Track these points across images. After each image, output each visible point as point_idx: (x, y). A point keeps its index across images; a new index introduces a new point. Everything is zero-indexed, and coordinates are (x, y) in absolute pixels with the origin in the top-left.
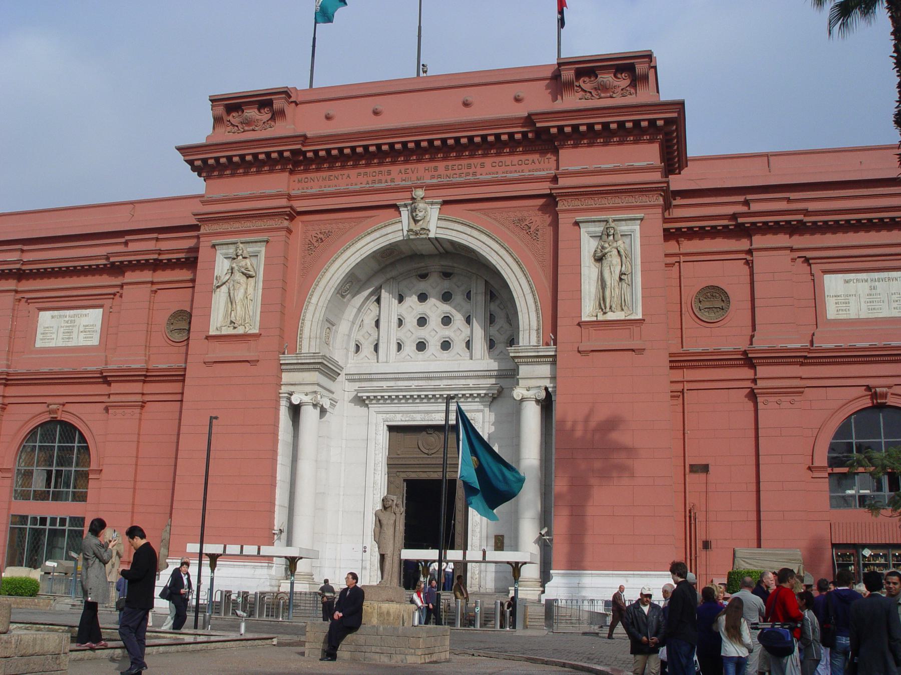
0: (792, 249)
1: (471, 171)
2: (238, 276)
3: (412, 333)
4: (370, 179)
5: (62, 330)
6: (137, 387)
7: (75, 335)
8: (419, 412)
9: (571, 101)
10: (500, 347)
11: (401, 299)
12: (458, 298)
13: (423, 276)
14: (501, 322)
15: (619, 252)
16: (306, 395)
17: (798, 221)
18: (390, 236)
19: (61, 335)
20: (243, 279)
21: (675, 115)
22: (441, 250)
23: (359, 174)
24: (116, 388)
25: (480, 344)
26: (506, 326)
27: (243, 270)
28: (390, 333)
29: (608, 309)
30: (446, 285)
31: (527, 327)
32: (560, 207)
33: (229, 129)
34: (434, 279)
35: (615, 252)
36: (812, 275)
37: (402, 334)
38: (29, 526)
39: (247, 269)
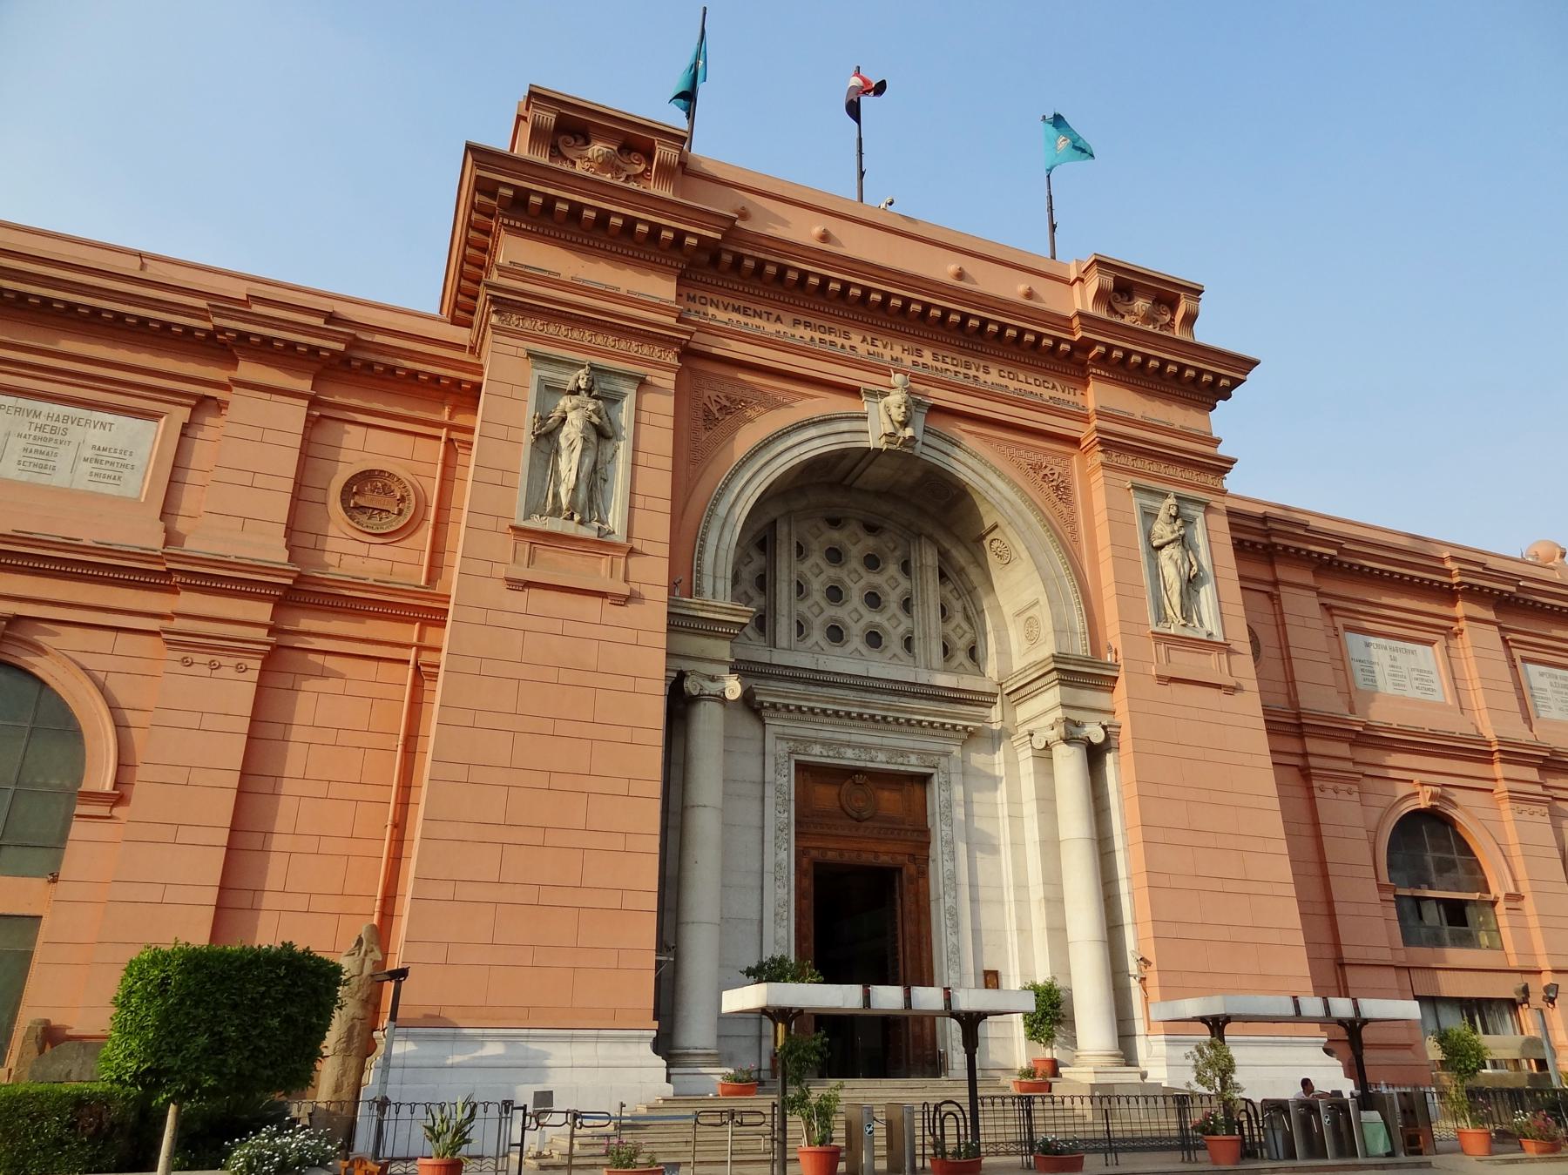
0: (1320, 594)
1: (972, 372)
4: (817, 335)
6: (262, 611)
8: (849, 745)
13: (835, 523)
14: (958, 618)
16: (713, 679)
17: (1332, 556)
18: (846, 437)
20: (593, 438)
21: (1240, 376)
23: (796, 322)
25: (937, 649)
26: (965, 626)
27: (595, 419)
30: (869, 543)
34: (854, 527)
36: (1336, 629)
37: (803, 607)
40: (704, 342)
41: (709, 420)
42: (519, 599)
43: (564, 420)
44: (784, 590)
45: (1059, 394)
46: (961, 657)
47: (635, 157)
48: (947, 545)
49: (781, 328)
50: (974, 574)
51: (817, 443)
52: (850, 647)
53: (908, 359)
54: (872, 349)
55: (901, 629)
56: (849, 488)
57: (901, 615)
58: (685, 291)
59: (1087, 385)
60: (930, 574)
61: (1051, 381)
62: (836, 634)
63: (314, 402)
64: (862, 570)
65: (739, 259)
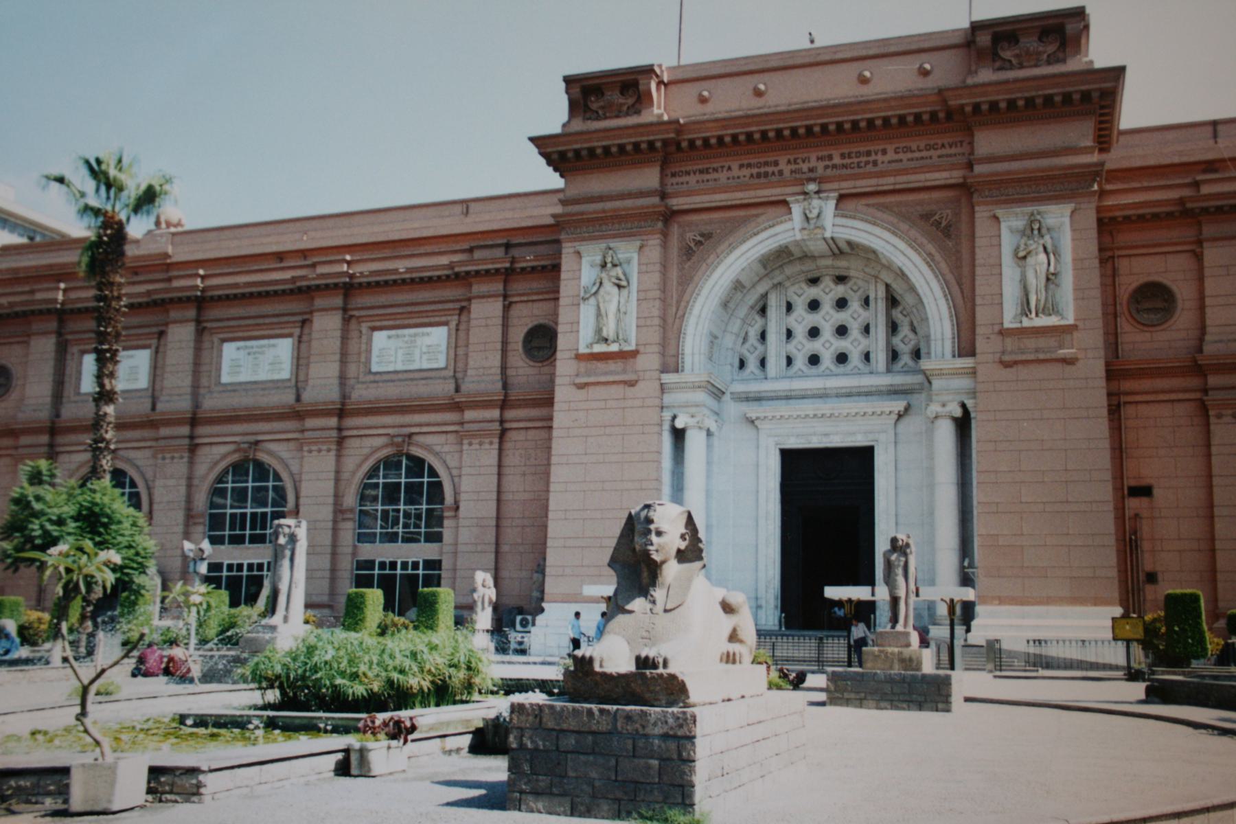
1: (873, 157)
2: (609, 287)
3: (802, 347)
4: (755, 171)
5: (400, 352)
6: (496, 413)
7: (417, 356)
9: (986, 75)
10: (906, 359)
11: (789, 307)
12: (855, 305)
13: (814, 281)
15: (1045, 248)
18: (779, 237)
19: (400, 357)
20: (616, 289)
22: (836, 251)
23: (741, 166)
24: (469, 415)
26: (911, 335)
28: (775, 348)
29: (1033, 314)
30: (840, 291)
31: (939, 336)
32: (976, 198)
33: (588, 115)
34: (827, 282)
35: (1041, 249)
37: (791, 348)
38: (376, 572)
39: (619, 279)
40: (677, 203)
41: (688, 253)
42: (582, 394)
43: (601, 283)
44: (772, 337)
45: (948, 151)
46: (906, 359)
47: (631, 92)
48: (889, 281)
49: (730, 174)
50: (909, 299)
51: (760, 247)
53: (821, 165)
54: (793, 167)
55: (861, 348)
58: (668, 172)
59: (972, 135)
60: (879, 301)
61: (940, 142)
62: (814, 360)
63: (505, 297)
64: (832, 312)
65: (692, 143)
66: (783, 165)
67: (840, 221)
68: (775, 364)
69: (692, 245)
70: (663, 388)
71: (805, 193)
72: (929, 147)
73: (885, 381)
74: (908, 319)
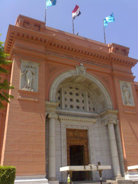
3: (69, 103)
13: (71, 88)
14: (91, 103)
16: (53, 115)
20: (32, 74)
23: (64, 55)
26: (93, 105)
27: (32, 72)
30: (77, 91)
34: (74, 89)
44: (63, 99)
46: (92, 110)
51: (68, 75)
52: (74, 109)
53: (82, 60)
56: (73, 82)
57: (82, 103)
62: (72, 107)
66: (74, 58)
67: (87, 74)
68: (63, 106)
69: (52, 69)
70: (46, 106)
71: (80, 66)
72: (104, 64)
73: (90, 114)
74: (91, 101)
